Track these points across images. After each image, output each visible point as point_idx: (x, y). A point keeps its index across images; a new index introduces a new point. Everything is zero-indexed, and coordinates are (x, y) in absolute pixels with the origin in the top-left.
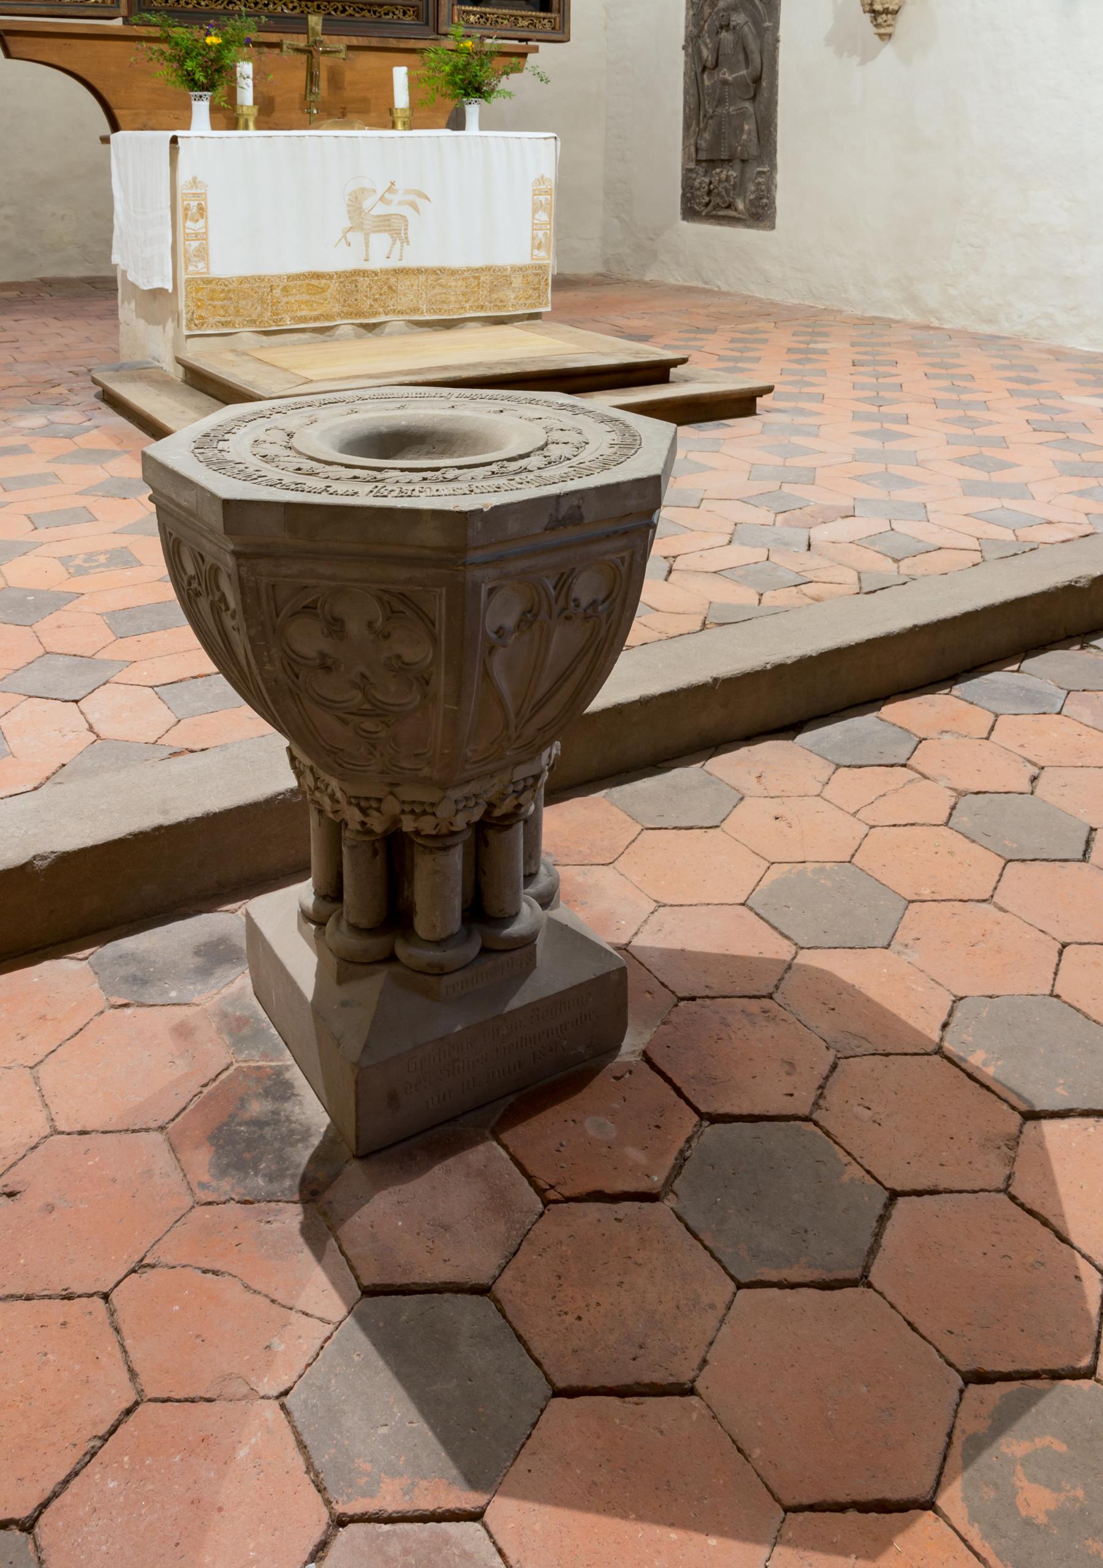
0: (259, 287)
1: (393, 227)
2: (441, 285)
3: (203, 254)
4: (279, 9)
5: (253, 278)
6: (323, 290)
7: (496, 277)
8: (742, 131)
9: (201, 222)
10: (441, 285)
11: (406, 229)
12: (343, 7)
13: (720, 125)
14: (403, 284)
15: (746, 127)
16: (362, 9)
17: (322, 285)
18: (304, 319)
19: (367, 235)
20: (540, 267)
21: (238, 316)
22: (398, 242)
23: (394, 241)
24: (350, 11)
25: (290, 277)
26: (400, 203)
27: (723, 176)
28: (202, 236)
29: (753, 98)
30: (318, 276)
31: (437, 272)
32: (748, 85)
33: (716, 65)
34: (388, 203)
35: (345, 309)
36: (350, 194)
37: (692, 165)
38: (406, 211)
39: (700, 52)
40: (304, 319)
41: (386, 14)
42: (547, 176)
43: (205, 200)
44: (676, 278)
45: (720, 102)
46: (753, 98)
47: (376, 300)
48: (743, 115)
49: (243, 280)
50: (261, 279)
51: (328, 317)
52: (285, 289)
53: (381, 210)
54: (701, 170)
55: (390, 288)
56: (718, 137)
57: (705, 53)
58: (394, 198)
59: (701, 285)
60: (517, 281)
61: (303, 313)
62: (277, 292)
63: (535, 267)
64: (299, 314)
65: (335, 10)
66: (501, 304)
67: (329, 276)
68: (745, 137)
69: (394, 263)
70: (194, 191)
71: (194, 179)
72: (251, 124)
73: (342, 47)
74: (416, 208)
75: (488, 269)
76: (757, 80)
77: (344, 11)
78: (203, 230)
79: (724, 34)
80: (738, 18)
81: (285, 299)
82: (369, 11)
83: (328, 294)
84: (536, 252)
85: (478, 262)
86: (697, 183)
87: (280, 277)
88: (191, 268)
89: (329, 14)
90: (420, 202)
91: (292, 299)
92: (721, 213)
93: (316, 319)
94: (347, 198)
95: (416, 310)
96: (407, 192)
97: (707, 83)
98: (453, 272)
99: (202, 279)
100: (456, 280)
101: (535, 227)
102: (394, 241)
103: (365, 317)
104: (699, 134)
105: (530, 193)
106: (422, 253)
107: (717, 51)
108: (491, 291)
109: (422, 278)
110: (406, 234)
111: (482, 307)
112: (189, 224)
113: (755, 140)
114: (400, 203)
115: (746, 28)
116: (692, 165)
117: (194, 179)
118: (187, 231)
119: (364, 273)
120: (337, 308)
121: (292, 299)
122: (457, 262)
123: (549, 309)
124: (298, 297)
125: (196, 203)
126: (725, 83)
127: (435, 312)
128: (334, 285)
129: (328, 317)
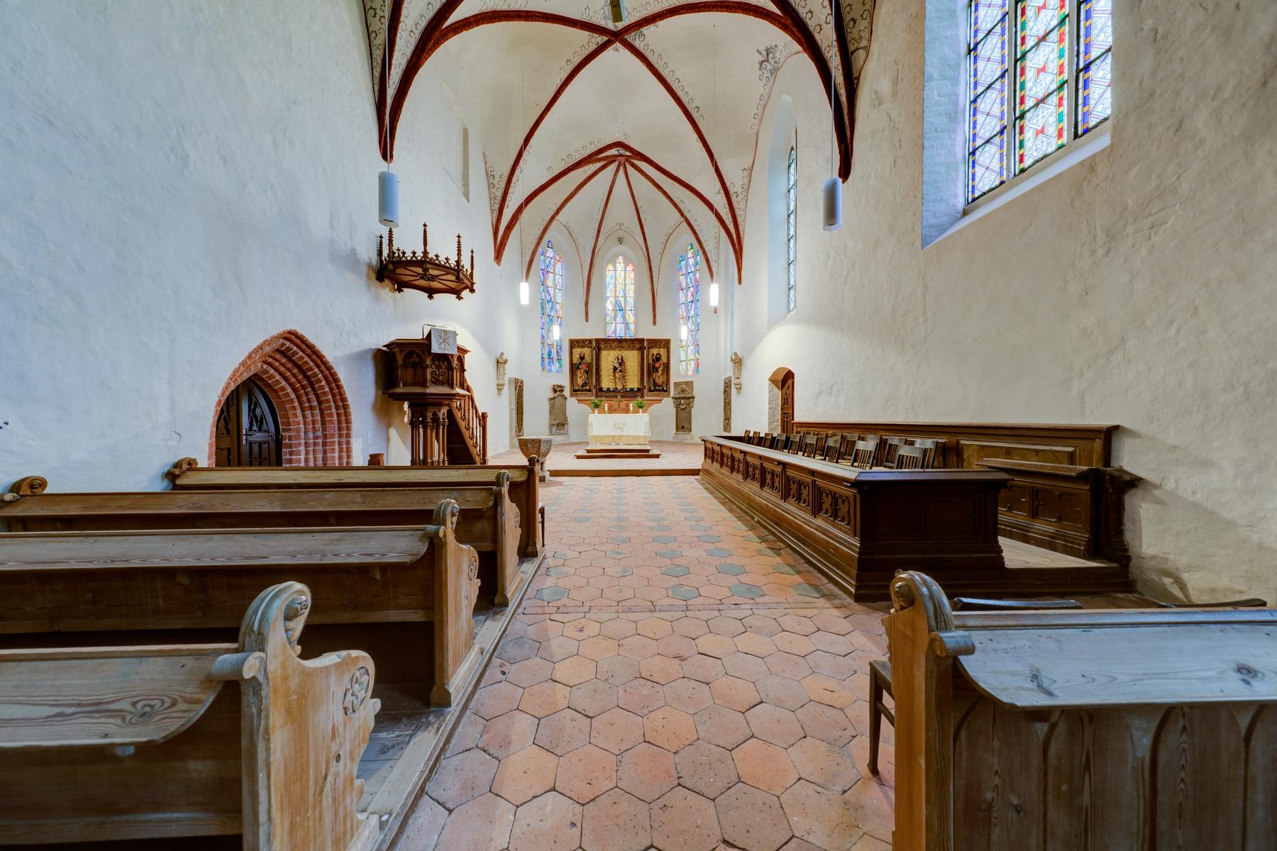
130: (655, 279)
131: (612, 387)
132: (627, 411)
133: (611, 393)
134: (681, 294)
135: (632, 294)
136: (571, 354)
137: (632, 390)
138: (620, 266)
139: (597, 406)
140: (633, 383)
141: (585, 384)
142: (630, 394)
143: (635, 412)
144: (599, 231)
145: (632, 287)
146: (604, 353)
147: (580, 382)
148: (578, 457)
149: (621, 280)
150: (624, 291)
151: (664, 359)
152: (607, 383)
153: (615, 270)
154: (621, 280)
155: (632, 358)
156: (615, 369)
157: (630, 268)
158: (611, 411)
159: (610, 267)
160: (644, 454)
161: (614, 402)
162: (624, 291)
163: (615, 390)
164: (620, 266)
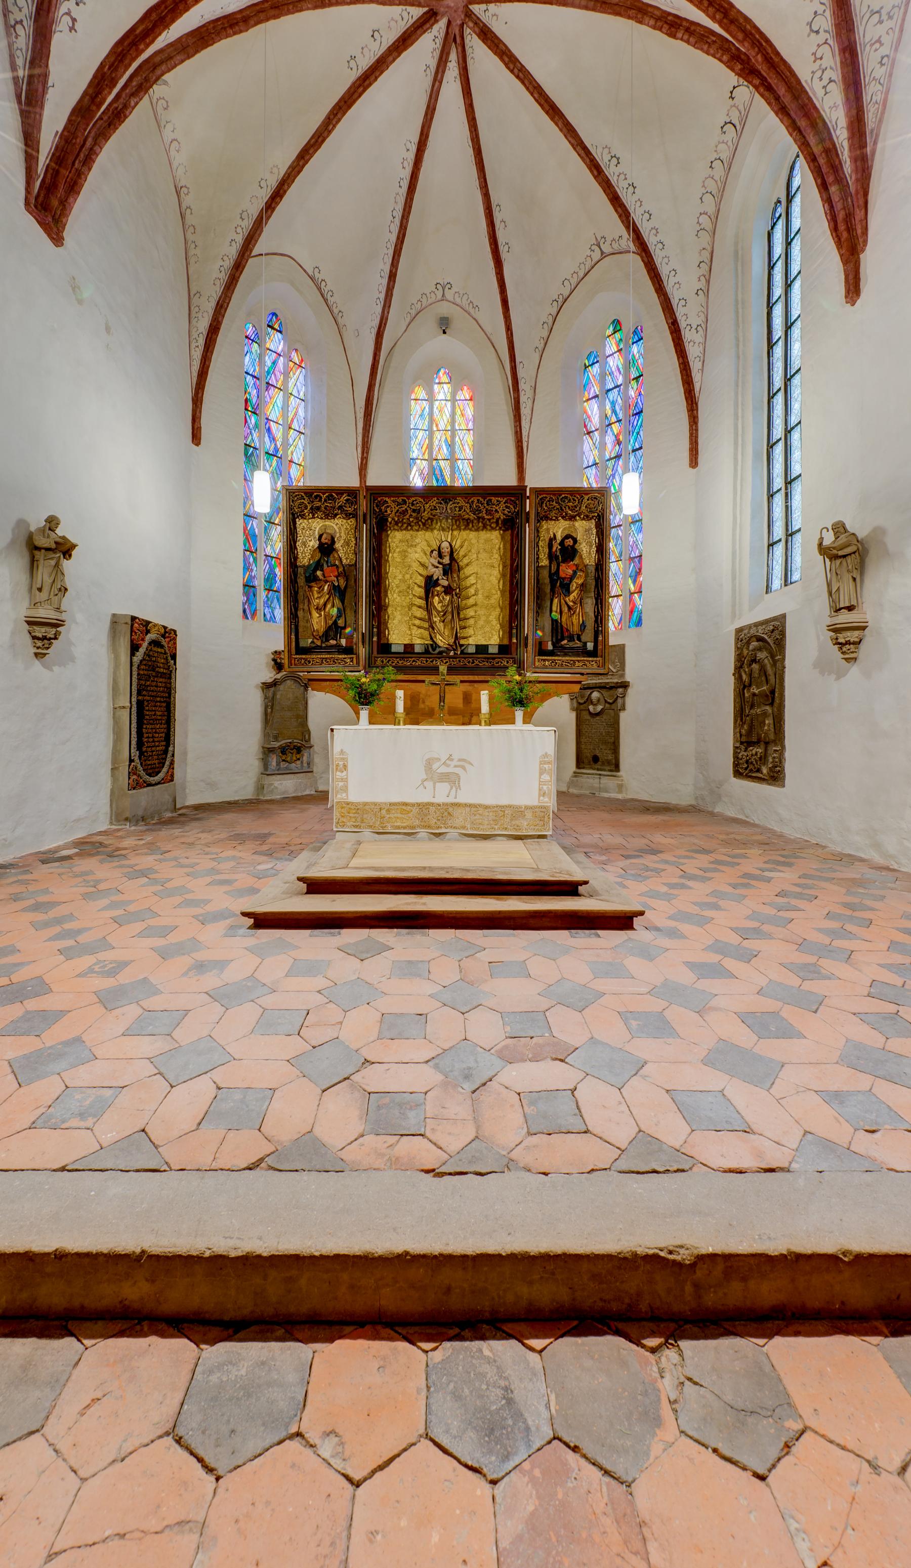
1: (452, 780)
6: (408, 812)
7: (518, 812)
8: (765, 724)
9: (345, 773)
13: (752, 720)
14: (457, 812)
15: (767, 722)
19: (434, 784)
23: (452, 788)
24: (476, 662)
26: (455, 766)
27: (754, 752)
29: (772, 704)
30: (406, 804)
32: (767, 696)
33: (750, 685)
34: (448, 766)
37: (738, 745)
38: (458, 771)
39: (741, 676)
40: (398, 827)
42: (549, 753)
44: (731, 813)
45: (752, 706)
46: (772, 704)
48: (765, 714)
50: (375, 804)
51: (413, 828)
52: (388, 811)
53: (443, 769)
54: (743, 747)
55: (449, 813)
56: (751, 727)
57: (744, 677)
58: (453, 763)
59: (744, 818)
60: (529, 815)
61: (398, 824)
62: (384, 812)
67: (413, 805)
68: (766, 728)
69: (451, 800)
71: (342, 751)
73: (458, 681)
75: (510, 806)
76: (773, 692)
79: (754, 665)
80: (761, 655)
83: (411, 815)
84: (542, 798)
86: (740, 756)
90: (467, 766)
91: (391, 816)
92: (754, 775)
93: (404, 828)
96: (460, 760)
97: (746, 695)
98: (487, 807)
101: (541, 783)
102: (452, 788)
104: (742, 726)
105: (538, 763)
107: (750, 675)
108: (511, 820)
112: (338, 773)
113: (773, 730)
114: (455, 766)
115: (766, 661)
116: (738, 745)
119: (432, 804)
120: (417, 822)
121: (391, 816)
126: (754, 695)
127: (475, 829)
128: (415, 810)
129: (413, 828)
130: (525, 411)
131: (419, 640)
132: (467, 714)
133: (415, 663)
134: (587, 443)
135: (469, 454)
137: (482, 649)
138: (442, 391)
139: (364, 697)
140: (485, 629)
141: (334, 630)
142: (477, 664)
143: (498, 717)
144: (392, 276)
145: (469, 438)
146: (396, 539)
147: (318, 622)
149: (443, 421)
150: (451, 446)
152: (402, 630)
153: (431, 399)
154: (443, 421)
155: (483, 556)
156: (430, 584)
157: (465, 394)
158: (417, 714)
159: (420, 393)
161: (427, 689)
162: (451, 446)
163: (431, 650)
164: (442, 391)
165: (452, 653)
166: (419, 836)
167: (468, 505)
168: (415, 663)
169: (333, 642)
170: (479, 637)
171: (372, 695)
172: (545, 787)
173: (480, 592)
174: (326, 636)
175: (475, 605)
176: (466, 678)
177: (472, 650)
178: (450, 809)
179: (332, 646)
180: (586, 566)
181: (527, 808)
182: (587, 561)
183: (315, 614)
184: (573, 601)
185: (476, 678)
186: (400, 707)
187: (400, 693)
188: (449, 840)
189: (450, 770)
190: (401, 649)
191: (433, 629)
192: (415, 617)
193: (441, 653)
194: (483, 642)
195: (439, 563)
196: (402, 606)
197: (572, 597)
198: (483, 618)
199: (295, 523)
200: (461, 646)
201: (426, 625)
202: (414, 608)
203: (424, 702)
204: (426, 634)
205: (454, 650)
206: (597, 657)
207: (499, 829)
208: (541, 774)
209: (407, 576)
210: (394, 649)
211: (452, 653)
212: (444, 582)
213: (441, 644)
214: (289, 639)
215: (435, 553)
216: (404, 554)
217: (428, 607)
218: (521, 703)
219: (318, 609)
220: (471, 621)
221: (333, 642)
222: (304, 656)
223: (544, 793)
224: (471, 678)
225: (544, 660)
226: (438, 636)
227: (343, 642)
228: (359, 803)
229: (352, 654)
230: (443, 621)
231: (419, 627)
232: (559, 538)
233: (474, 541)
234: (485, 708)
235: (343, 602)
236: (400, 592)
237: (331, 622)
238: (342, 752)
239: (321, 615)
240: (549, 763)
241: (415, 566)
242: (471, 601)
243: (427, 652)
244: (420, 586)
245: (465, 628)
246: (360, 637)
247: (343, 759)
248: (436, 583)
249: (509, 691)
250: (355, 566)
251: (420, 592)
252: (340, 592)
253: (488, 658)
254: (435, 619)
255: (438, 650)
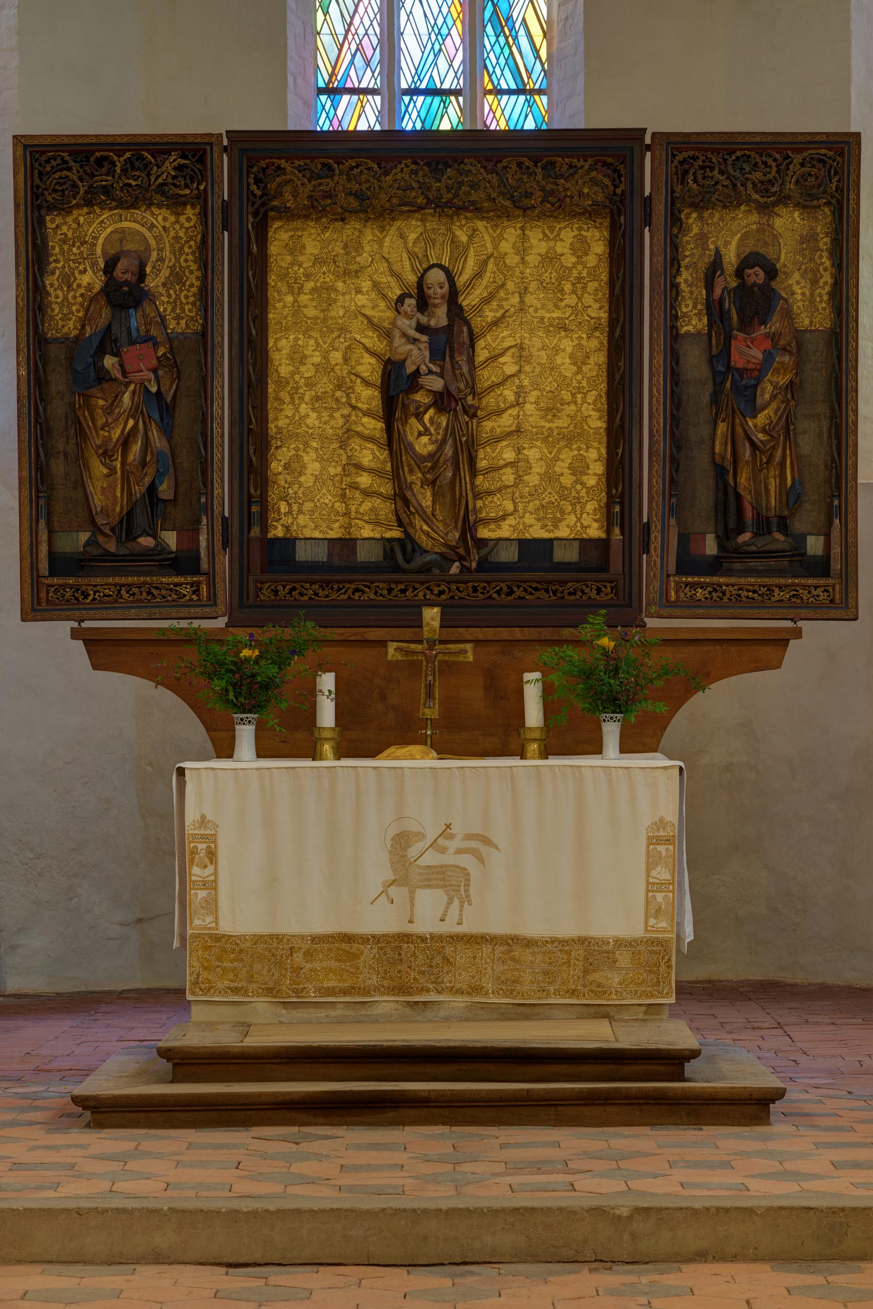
0: (276, 948)
1: (451, 882)
2: (514, 960)
3: (212, 906)
4: (421, 595)
5: (271, 936)
6: (356, 956)
9: (210, 869)
10: (514, 960)
11: (467, 885)
12: (509, 587)
16: (536, 589)
17: (353, 950)
18: (331, 992)
19: (412, 893)
20: (659, 942)
21: (249, 982)
22: (456, 902)
23: (450, 901)
24: (519, 593)
25: (315, 939)
26: (459, 851)
28: (212, 885)
30: (348, 938)
31: (511, 941)
34: (443, 850)
35: (386, 983)
36: (393, 839)
38: (467, 861)
40: (331, 992)
41: (570, 594)
43: (215, 842)
47: (423, 973)
49: (259, 939)
50: (278, 938)
51: (366, 992)
52: (309, 955)
53: (431, 859)
55: (446, 960)
60: (624, 959)
61: (332, 984)
62: (298, 957)
63: (652, 942)
64: (326, 984)
65: (498, 592)
66: (600, 989)
67: (364, 939)
69: (450, 927)
70: (202, 832)
71: (203, 817)
72: (327, 748)
74: (481, 859)
75: (582, 941)
77: (511, 592)
78: (212, 878)
81: (309, 966)
82: (547, 591)
84: (652, 921)
85: (567, 929)
87: (302, 937)
88: (197, 922)
89: (490, 597)
91: (317, 965)
94: (389, 843)
95: (476, 989)
98: (529, 943)
99: (210, 936)
100: (533, 954)
102: (450, 901)
103: (410, 994)
106: (490, 915)
108: (586, 972)
109: (487, 949)
110: (467, 891)
111: (574, 991)
114: (459, 851)
117: (203, 817)
118: (193, 878)
119: (405, 938)
120: (374, 980)
121: (317, 965)
122: (535, 929)
123: (672, 1000)
124: (325, 964)
125: (204, 846)
128: (369, 953)
136: (34, 258)
137: (535, 551)
143: (570, 736)
148: (103, 1112)
151: (803, 296)
152: (325, 485)
156: (396, 387)
160: (639, 1087)
163: (400, 553)
165: (455, 569)
166: (377, 1010)
167: (494, 179)
168: (360, 589)
169: (146, 542)
170: (529, 519)
171: (265, 686)
172: (660, 897)
173: (533, 396)
174: (127, 527)
175: (518, 431)
176: (490, 633)
177: (509, 555)
178: (449, 950)
179: (145, 555)
180: (799, 335)
181: (620, 943)
182: (804, 322)
183: (99, 469)
184: (764, 431)
185: (517, 633)
186: (327, 715)
187: (327, 681)
188: (446, 1019)
189: (449, 859)
190: (320, 554)
191: (407, 502)
192: (359, 467)
193: (426, 569)
194: (538, 532)
195: (421, 328)
196: (323, 437)
197: (761, 419)
198: (538, 468)
199: (41, 222)
200: (482, 543)
201: (386, 488)
202: (355, 443)
203: (383, 698)
204: (386, 509)
205: (461, 558)
206: (826, 573)
207: (557, 992)
208: (649, 868)
209: (336, 357)
210: (303, 554)
211: (455, 569)
212: (432, 374)
213: (425, 542)
214: (34, 533)
215: (410, 303)
216: (325, 296)
217: (393, 441)
218: (614, 703)
219: (106, 455)
220: (508, 477)
221: (146, 542)
222: (71, 581)
223: (658, 910)
224: (505, 633)
225: (693, 586)
226: (418, 522)
227: (171, 539)
228: (243, 938)
229: (197, 571)
230: (433, 483)
231: (367, 493)
232: (731, 258)
233: (512, 260)
234: (534, 715)
235: (167, 432)
236: (317, 398)
237: (138, 490)
238: (203, 821)
239: (113, 471)
240: (668, 841)
241: (357, 326)
242: (506, 421)
243: (389, 554)
244: (366, 383)
245: (490, 493)
246: (218, 527)
247: (204, 838)
248: (413, 381)
249: (587, 674)
250: (204, 337)
251: (369, 397)
252: (161, 407)
253: (550, 582)
254: (410, 478)
255: (419, 561)
